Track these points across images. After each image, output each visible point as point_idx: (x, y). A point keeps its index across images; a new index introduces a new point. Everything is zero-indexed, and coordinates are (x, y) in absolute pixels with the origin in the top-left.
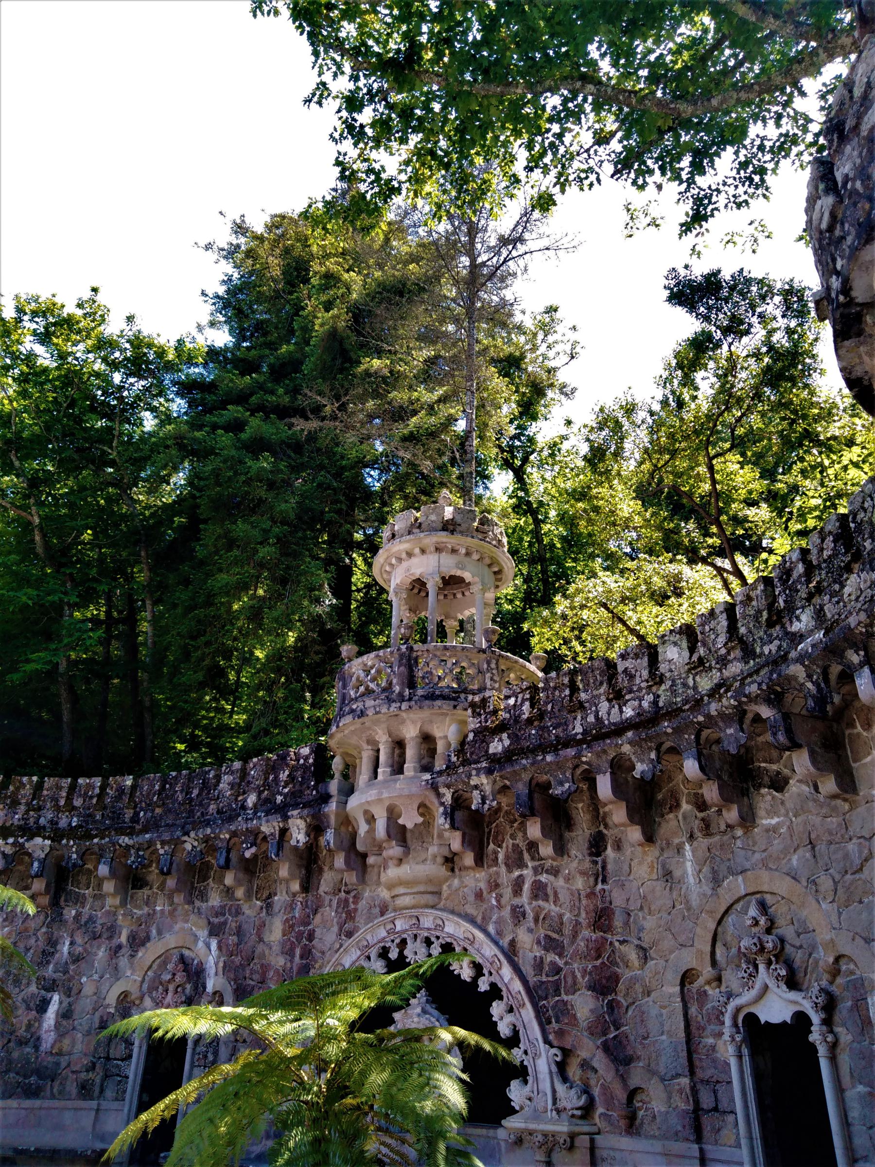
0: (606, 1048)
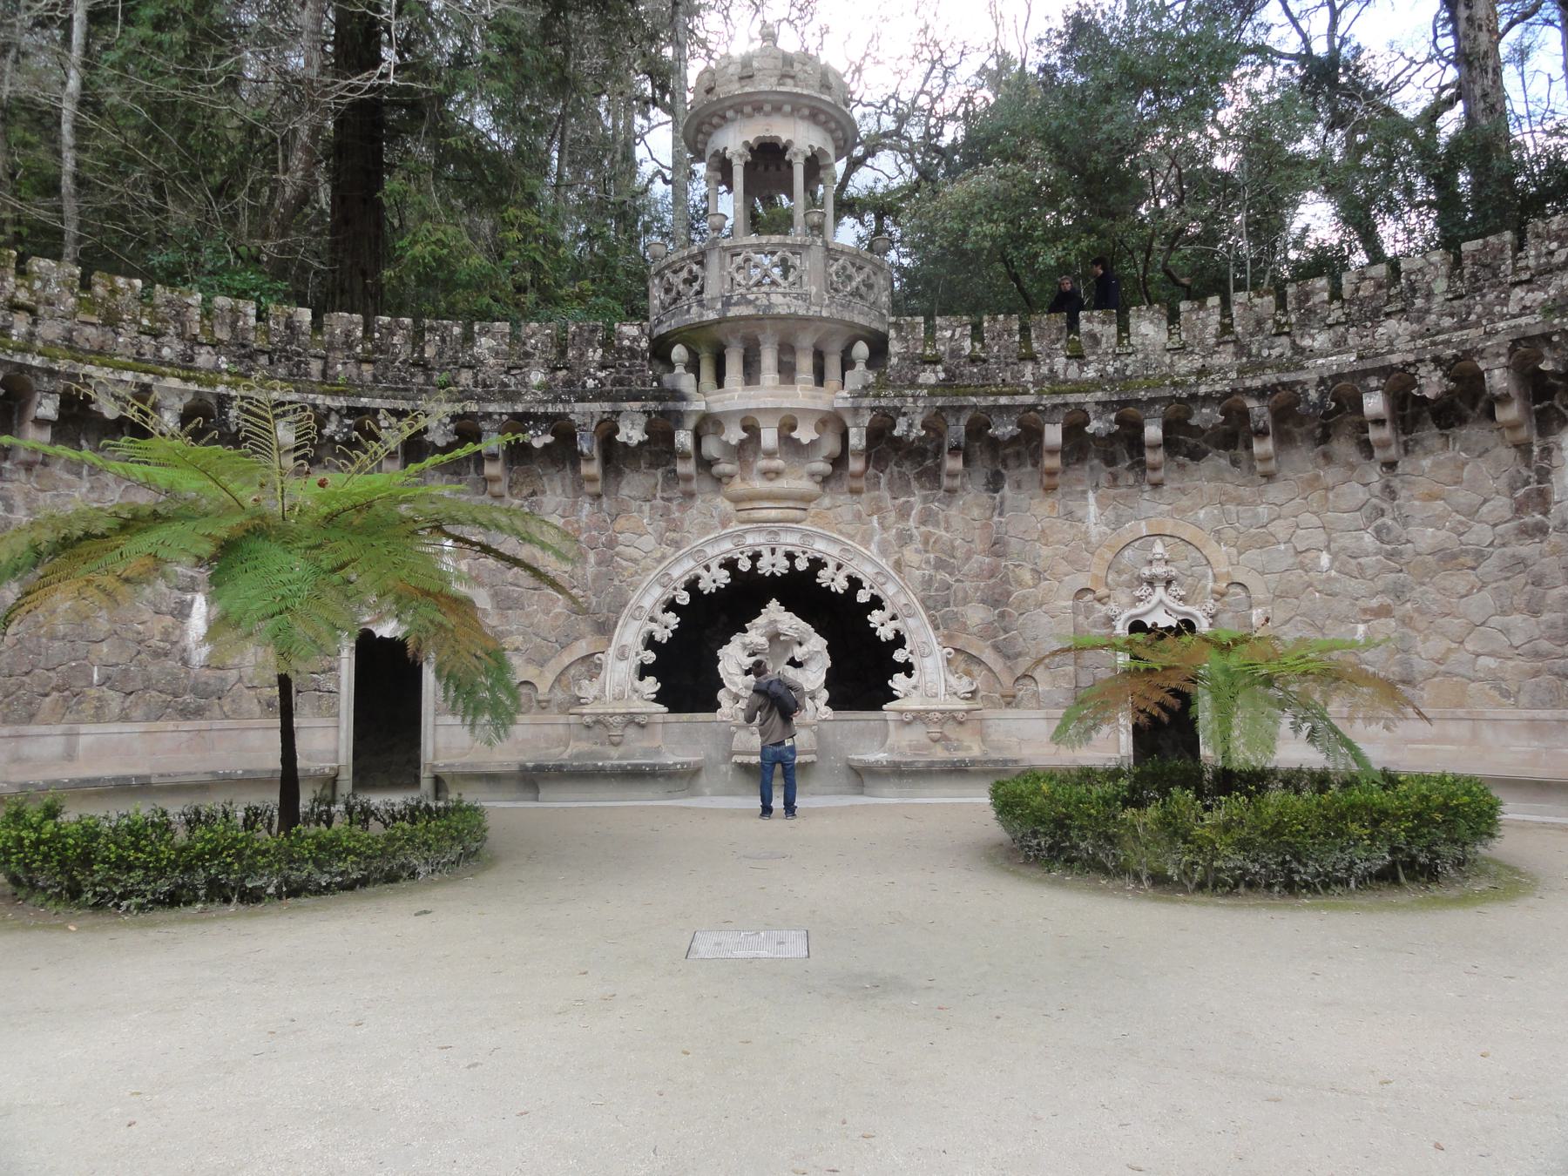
0: (996, 648)
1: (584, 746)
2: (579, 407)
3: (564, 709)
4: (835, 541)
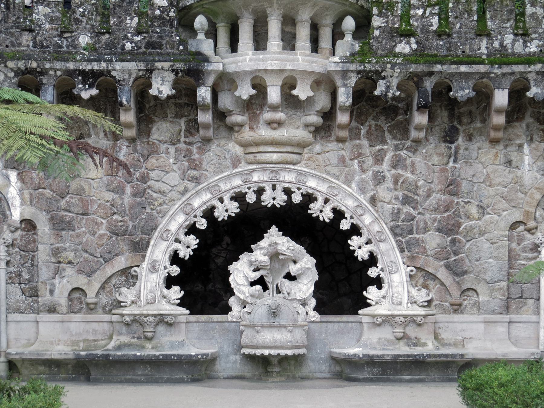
0: (447, 266)
1: (125, 339)
2: (118, 66)
3: (107, 310)
4: (324, 180)
